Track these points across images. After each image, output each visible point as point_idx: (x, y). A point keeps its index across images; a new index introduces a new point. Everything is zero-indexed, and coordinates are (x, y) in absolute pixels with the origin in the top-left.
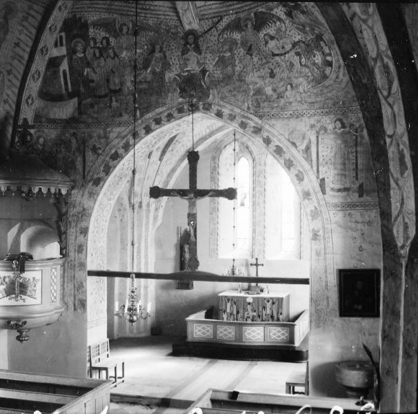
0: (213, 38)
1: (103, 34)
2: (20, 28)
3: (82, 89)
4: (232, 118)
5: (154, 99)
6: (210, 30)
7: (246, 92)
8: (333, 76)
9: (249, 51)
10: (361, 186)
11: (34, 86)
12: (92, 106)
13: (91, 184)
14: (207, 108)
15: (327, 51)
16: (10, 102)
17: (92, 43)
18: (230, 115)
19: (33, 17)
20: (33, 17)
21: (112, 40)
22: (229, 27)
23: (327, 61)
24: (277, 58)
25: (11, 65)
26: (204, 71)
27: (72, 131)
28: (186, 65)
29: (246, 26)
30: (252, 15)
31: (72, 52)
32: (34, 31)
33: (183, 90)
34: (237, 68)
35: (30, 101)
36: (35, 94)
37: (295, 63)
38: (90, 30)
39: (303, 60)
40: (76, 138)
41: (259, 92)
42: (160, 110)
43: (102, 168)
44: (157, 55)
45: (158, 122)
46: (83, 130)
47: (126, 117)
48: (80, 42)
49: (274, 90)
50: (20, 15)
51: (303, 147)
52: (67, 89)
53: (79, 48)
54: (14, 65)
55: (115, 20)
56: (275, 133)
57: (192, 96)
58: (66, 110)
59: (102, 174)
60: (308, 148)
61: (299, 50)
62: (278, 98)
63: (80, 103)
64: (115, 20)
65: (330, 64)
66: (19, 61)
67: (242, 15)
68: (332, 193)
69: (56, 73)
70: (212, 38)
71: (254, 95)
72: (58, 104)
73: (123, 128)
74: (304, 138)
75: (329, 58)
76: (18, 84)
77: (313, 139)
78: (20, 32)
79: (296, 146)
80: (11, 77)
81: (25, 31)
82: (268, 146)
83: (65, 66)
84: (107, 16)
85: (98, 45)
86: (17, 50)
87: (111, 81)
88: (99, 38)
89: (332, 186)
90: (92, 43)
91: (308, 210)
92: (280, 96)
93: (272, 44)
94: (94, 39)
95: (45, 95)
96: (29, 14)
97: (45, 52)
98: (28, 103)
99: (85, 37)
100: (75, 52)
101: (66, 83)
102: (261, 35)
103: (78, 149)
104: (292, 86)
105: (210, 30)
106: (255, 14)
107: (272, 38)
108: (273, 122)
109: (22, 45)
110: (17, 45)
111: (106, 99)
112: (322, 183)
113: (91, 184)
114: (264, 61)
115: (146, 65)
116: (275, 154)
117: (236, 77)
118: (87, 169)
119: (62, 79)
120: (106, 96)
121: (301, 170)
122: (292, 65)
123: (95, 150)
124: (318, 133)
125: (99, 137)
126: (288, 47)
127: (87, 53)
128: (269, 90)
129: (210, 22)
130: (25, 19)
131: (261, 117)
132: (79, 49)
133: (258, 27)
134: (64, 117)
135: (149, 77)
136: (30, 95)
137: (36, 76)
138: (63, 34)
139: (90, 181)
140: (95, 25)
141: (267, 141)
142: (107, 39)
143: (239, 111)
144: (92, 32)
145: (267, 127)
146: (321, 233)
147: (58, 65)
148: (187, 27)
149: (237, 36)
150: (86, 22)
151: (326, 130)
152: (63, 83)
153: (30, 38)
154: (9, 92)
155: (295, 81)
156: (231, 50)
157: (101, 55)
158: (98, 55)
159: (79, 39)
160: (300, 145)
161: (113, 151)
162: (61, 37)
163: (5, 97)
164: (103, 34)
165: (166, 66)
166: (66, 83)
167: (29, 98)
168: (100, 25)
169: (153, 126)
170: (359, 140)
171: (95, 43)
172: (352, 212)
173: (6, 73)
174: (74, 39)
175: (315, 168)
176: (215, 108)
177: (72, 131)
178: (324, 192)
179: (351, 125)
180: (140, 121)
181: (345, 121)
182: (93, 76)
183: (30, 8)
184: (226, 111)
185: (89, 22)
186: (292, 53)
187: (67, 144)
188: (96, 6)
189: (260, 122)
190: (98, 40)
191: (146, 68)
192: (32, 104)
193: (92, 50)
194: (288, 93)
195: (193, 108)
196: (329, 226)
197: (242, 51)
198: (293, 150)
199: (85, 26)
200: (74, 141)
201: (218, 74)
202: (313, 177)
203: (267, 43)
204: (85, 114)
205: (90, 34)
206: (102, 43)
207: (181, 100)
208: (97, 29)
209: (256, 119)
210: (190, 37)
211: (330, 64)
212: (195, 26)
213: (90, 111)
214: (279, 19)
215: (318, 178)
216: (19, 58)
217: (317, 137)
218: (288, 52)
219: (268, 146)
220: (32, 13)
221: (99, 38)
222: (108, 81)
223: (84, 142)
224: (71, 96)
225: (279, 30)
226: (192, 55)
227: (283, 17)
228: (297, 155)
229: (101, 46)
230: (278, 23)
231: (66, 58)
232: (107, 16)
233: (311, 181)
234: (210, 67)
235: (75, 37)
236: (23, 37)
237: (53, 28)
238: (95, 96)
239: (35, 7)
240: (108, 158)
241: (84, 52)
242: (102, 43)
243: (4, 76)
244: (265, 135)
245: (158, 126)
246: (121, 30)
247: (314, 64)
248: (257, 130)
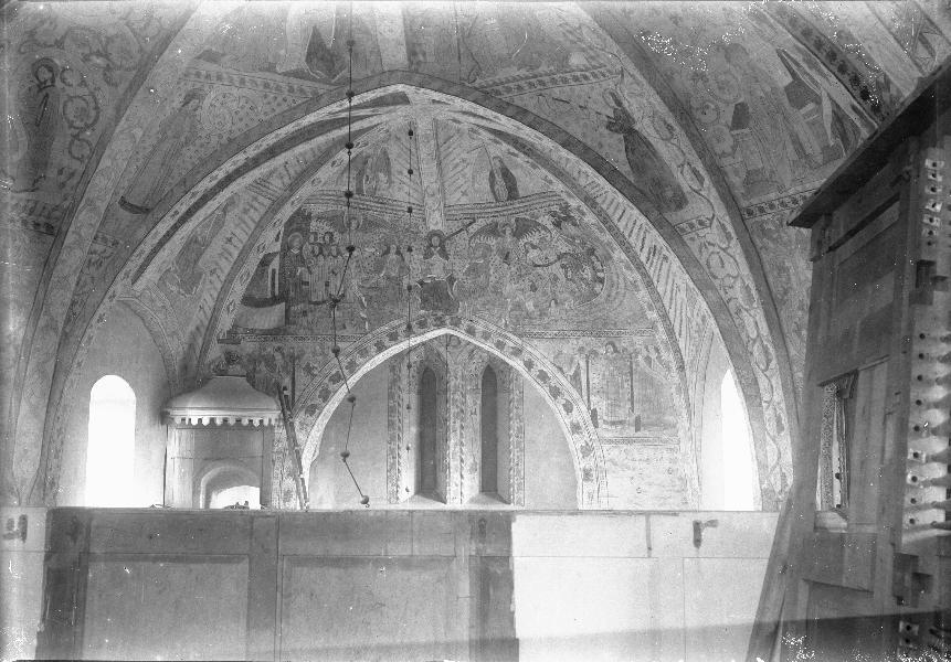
0: (462, 241)
3: (292, 294)
4: (486, 336)
5: (387, 308)
6: (459, 231)
7: (503, 306)
8: (604, 294)
9: (506, 257)
10: (638, 420)
11: (239, 289)
12: (305, 313)
13: (303, 412)
14: (456, 324)
15: (597, 264)
16: (206, 308)
17: (312, 240)
18: (484, 333)
19: (256, 209)
20: (256, 209)
21: (337, 236)
22: (479, 232)
23: (599, 278)
24: (539, 270)
25: (217, 264)
26: (451, 280)
27: (276, 345)
28: (429, 270)
29: (504, 232)
30: (513, 220)
31: (286, 248)
33: (425, 300)
34: (492, 278)
35: (231, 308)
37: (559, 276)
39: (570, 273)
40: (283, 354)
41: (518, 306)
42: (396, 322)
43: (318, 393)
44: (393, 256)
45: (394, 337)
46: (290, 344)
47: (349, 331)
48: (297, 236)
49: (535, 306)
50: (241, 207)
51: (572, 373)
52: (273, 293)
54: (220, 263)
56: (536, 353)
57: (436, 308)
58: (270, 317)
59: (319, 401)
60: (576, 378)
61: (565, 263)
62: (540, 315)
63: (287, 311)
65: (601, 281)
66: (226, 258)
67: (501, 220)
68: (604, 426)
70: (462, 242)
71: (512, 310)
72: (262, 310)
73: (348, 344)
74: (572, 361)
75: (600, 275)
76: (219, 286)
77: (583, 364)
78: (237, 226)
79: (563, 373)
80: (214, 278)
82: (529, 370)
83: (275, 264)
87: (332, 285)
89: (605, 418)
90: (312, 240)
91: (578, 446)
92: (542, 314)
93: (533, 254)
95: (248, 300)
96: (252, 206)
98: (228, 309)
99: (305, 232)
100: (289, 248)
101: (273, 285)
102: (521, 242)
103: (285, 368)
104: (556, 303)
105: (459, 231)
106: (517, 220)
107: (534, 247)
108: (536, 342)
110: (230, 240)
111: (325, 306)
112: (594, 415)
113: (303, 412)
114: (524, 272)
115: (379, 268)
116: (538, 380)
117: (490, 289)
118: (297, 393)
119: (270, 279)
120: (324, 302)
121: (570, 399)
122: (556, 279)
123: (309, 369)
124: (587, 357)
125: (314, 353)
126: (552, 259)
128: (530, 306)
129: (460, 224)
130: (246, 211)
131: (520, 336)
132: (295, 244)
133: (518, 234)
134: (266, 327)
135: (383, 283)
139: (303, 407)
140: (319, 218)
141: (529, 365)
142: (331, 234)
143: (495, 328)
145: (529, 349)
146: (593, 473)
148: (432, 227)
149: (492, 242)
151: (596, 353)
152: (269, 285)
155: (560, 297)
156: (484, 256)
157: (321, 252)
158: (317, 251)
160: (569, 370)
161: (334, 372)
164: (327, 228)
165: (404, 269)
166: (273, 285)
169: (386, 342)
170: (634, 367)
171: (316, 239)
172: (629, 447)
175: (586, 398)
176: (465, 324)
177: (276, 345)
178: (596, 426)
179: (625, 349)
180: (370, 335)
181: (617, 345)
182: (307, 277)
184: (480, 328)
186: (558, 264)
187: (270, 362)
189: (520, 342)
191: (378, 271)
194: (553, 309)
195: (440, 324)
196: (602, 464)
197: (498, 259)
198: (559, 375)
200: (278, 357)
201: (468, 284)
202: (584, 408)
203: (527, 252)
204: (294, 323)
207: (422, 312)
209: (516, 338)
210: (436, 238)
211: (601, 281)
212: (439, 227)
213: (303, 321)
214: (545, 228)
215: (589, 408)
217: (587, 362)
218: (552, 264)
219: (529, 370)
222: (327, 284)
223: (293, 358)
224: (275, 300)
225: (542, 240)
226: (436, 259)
227: (551, 227)
228: (564, 382)
230: (543, 232)
232: (335, 208)
233: (580, 412)
234: (460, 276)
236: (238, 231)
238: (310, 302)
239: (261, 199)
240: (326, 381)
241: (301, 248)
244: (526, 357)
245: (393, 342)
246: (349, 224)
247: (582, 279)
248: (517, 352)
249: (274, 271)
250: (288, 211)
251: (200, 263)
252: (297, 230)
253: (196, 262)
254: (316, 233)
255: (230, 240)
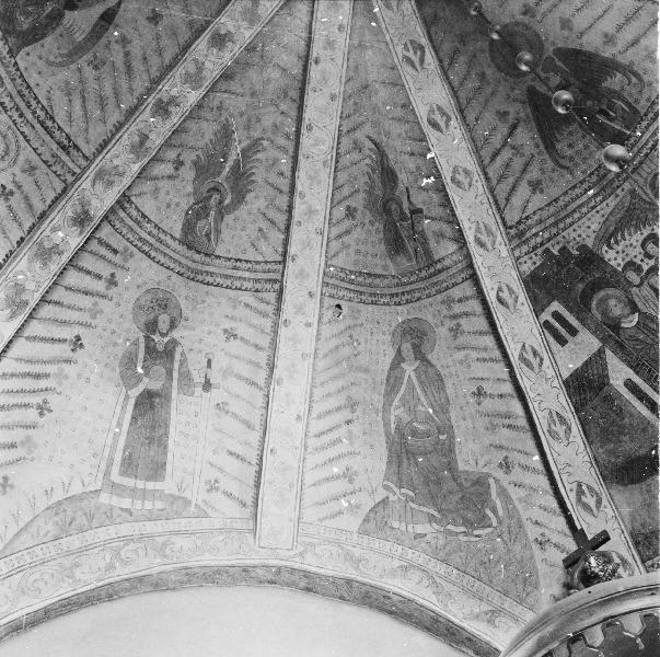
1: (637, 238)
2: (460, 355)
17: (634, 277)
19: (466, 314)
20: (466, 314)
31: (610, 331)
32: (489, 341)
35: (591, 501)
36: (590, 477)
38: (607, 257)
48: (608, 297)
50: (442, 332)
53: (616, 308)
55: (633, 192)
64: (633, 192)
66: (509, 426)
69: (610, 399)
78: (465, 362)
81: (474, 355)
83: (619, 373)
84: (612, 202)
85: (645, 268)
86: (487, 404)
88: (636, 253)
90: (634, 277)
94: (631, 265)
96: (455, 317)
97: (535, 362)
98: (586, 507)
99: (612, 279)
100: (615, 326)
109: (488, 387)
110: (480, 393)
127: (640, 305)
130: (456, 331)
136: (580, 485)
137: (560, 429)
138: (556, 306)
140: (609, 236)
144: (614, 257)
147: (603, 381)
150: (583, 248)
153: (491, 360)
154: (537, 514)
159: (602, 294)
162: (556, 315)
163: (533, 532)
164: (637, 238)
167: (580, 493)
168: (616, 230)
173: (499, 474)
174: (591, 299)
183: (449, 302)
185: (590, 243)
188: (574, 205)
190: (638, 261)
192: (599, 502)
193: (646, 290)
199: (589, 259)
205: (613, 263)
206: (649, 256)
208: (617, 242)
216: (507, 421)
220: (458, 308)
221: (636, 253)
229: (652, 262)
231: (608, 353)
235: (586, 298)
236: (480, 370)
237: (505, 295)
239: (457, 293)
241: (634, 308)
242: (649, 256)
243: (497, 481)
249: (629, 385)
250: (499, 269)
251: (461, 466)
252: (595, 287)
253: (451, 466)
254: (631, 265)
255: (480, 393)
